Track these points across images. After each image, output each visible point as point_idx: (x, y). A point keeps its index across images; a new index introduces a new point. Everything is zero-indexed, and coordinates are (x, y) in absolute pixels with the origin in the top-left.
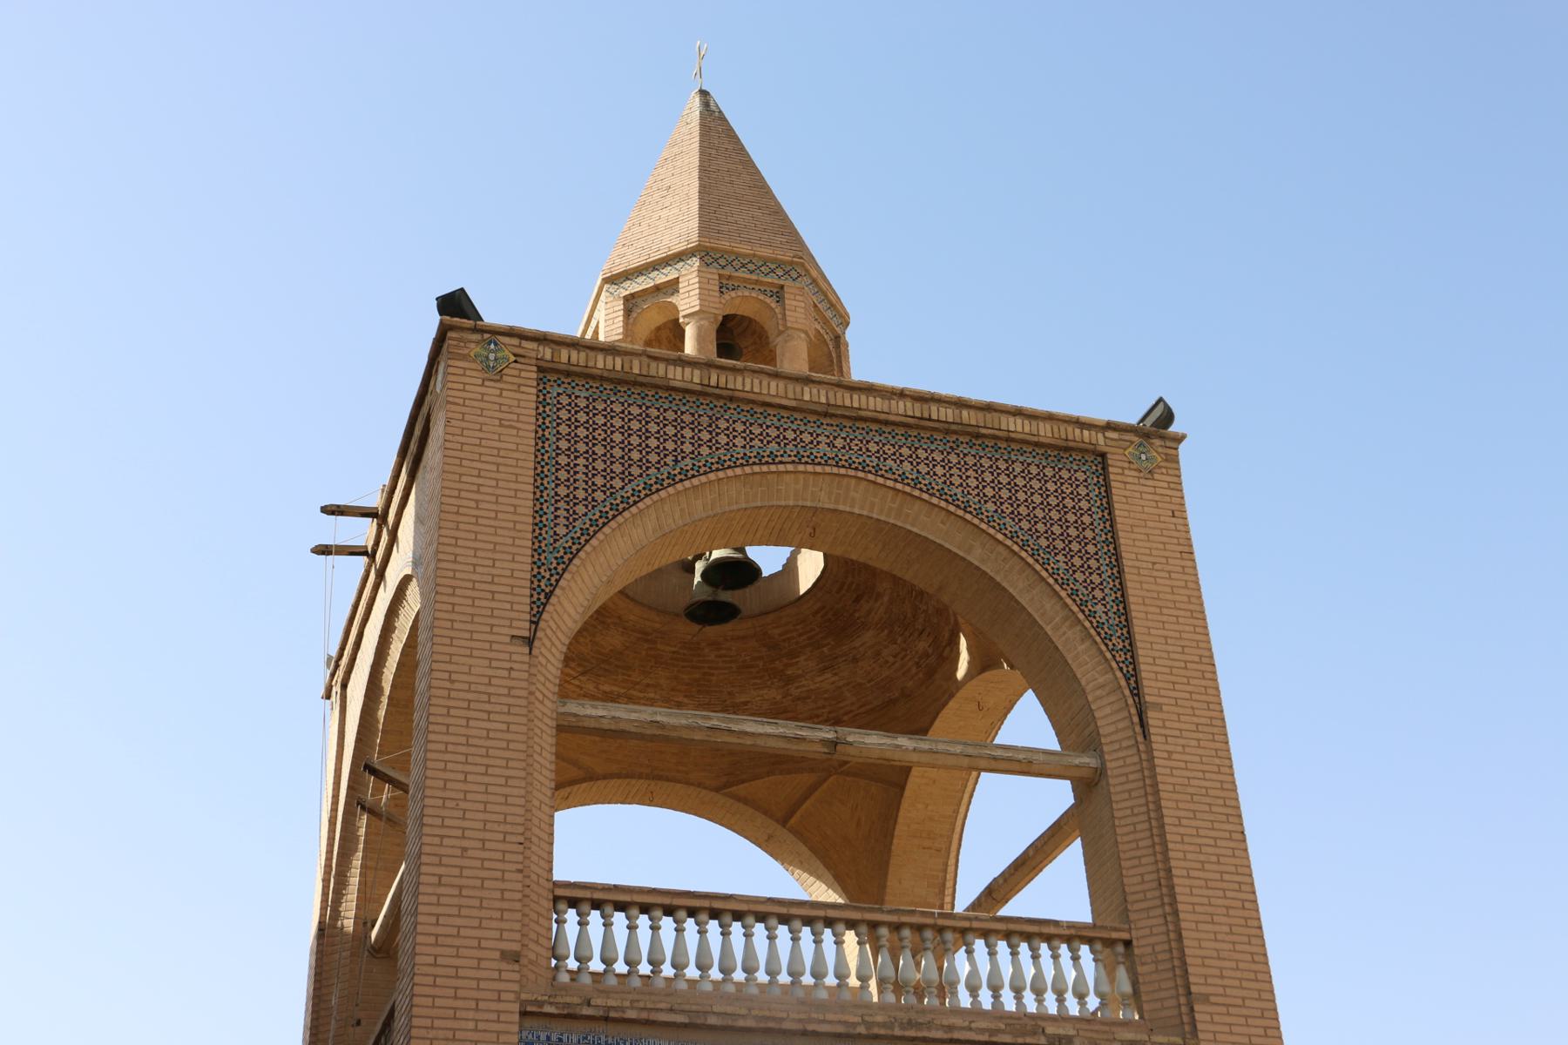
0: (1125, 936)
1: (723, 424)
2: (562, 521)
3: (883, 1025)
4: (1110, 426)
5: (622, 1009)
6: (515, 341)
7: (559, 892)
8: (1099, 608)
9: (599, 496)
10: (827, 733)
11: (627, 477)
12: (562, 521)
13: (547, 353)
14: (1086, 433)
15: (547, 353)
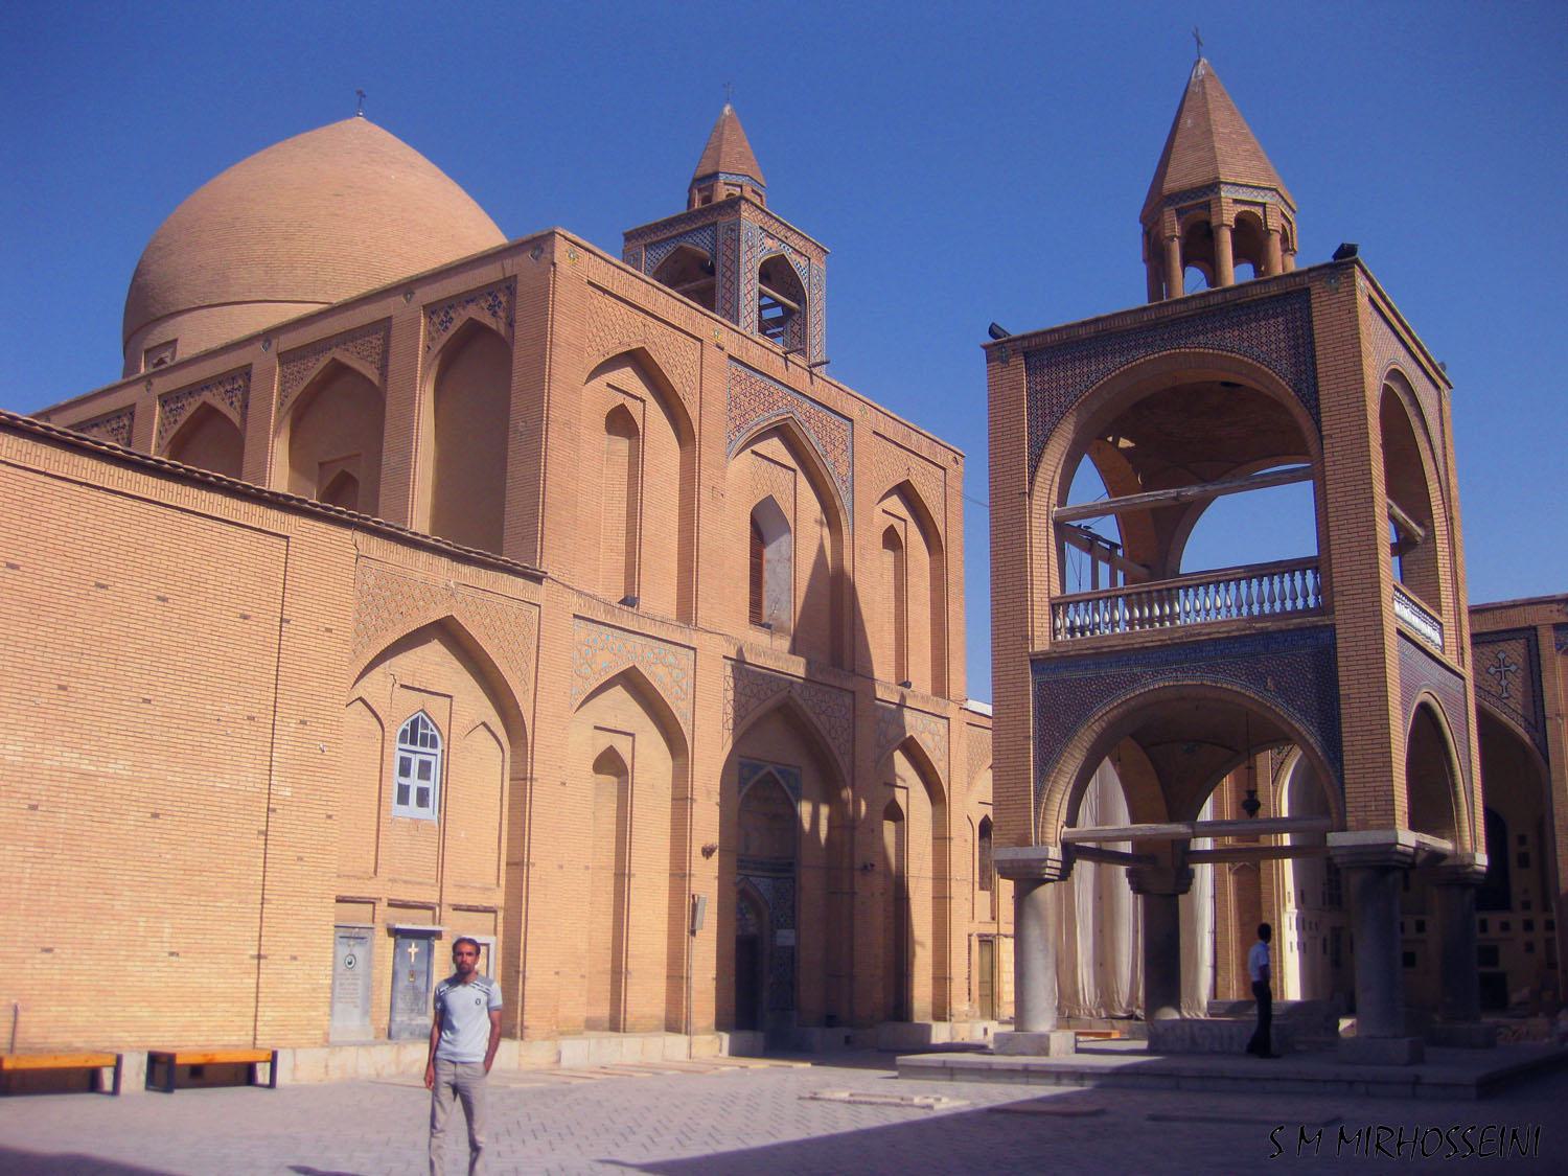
0: (1315, 565)
1: (1109, 348)
2: (1040, 428)
3: (1179, 638)
4: (1310, 270)
5: (1068, 651)
6: (1012, 344)
7: (1053, 602)
8: (1305, 385)
9: (1055, 409)
10: (1173, 492)
11: (1066, 395)
12: (1040, 428)
13: (1026, 344)
14: (1297, 279)
15: (1026, 344)
